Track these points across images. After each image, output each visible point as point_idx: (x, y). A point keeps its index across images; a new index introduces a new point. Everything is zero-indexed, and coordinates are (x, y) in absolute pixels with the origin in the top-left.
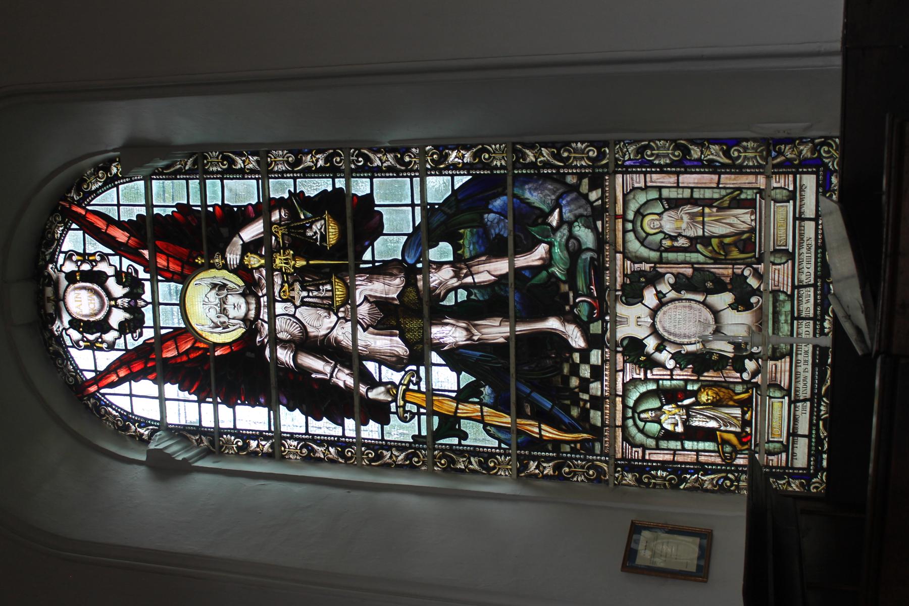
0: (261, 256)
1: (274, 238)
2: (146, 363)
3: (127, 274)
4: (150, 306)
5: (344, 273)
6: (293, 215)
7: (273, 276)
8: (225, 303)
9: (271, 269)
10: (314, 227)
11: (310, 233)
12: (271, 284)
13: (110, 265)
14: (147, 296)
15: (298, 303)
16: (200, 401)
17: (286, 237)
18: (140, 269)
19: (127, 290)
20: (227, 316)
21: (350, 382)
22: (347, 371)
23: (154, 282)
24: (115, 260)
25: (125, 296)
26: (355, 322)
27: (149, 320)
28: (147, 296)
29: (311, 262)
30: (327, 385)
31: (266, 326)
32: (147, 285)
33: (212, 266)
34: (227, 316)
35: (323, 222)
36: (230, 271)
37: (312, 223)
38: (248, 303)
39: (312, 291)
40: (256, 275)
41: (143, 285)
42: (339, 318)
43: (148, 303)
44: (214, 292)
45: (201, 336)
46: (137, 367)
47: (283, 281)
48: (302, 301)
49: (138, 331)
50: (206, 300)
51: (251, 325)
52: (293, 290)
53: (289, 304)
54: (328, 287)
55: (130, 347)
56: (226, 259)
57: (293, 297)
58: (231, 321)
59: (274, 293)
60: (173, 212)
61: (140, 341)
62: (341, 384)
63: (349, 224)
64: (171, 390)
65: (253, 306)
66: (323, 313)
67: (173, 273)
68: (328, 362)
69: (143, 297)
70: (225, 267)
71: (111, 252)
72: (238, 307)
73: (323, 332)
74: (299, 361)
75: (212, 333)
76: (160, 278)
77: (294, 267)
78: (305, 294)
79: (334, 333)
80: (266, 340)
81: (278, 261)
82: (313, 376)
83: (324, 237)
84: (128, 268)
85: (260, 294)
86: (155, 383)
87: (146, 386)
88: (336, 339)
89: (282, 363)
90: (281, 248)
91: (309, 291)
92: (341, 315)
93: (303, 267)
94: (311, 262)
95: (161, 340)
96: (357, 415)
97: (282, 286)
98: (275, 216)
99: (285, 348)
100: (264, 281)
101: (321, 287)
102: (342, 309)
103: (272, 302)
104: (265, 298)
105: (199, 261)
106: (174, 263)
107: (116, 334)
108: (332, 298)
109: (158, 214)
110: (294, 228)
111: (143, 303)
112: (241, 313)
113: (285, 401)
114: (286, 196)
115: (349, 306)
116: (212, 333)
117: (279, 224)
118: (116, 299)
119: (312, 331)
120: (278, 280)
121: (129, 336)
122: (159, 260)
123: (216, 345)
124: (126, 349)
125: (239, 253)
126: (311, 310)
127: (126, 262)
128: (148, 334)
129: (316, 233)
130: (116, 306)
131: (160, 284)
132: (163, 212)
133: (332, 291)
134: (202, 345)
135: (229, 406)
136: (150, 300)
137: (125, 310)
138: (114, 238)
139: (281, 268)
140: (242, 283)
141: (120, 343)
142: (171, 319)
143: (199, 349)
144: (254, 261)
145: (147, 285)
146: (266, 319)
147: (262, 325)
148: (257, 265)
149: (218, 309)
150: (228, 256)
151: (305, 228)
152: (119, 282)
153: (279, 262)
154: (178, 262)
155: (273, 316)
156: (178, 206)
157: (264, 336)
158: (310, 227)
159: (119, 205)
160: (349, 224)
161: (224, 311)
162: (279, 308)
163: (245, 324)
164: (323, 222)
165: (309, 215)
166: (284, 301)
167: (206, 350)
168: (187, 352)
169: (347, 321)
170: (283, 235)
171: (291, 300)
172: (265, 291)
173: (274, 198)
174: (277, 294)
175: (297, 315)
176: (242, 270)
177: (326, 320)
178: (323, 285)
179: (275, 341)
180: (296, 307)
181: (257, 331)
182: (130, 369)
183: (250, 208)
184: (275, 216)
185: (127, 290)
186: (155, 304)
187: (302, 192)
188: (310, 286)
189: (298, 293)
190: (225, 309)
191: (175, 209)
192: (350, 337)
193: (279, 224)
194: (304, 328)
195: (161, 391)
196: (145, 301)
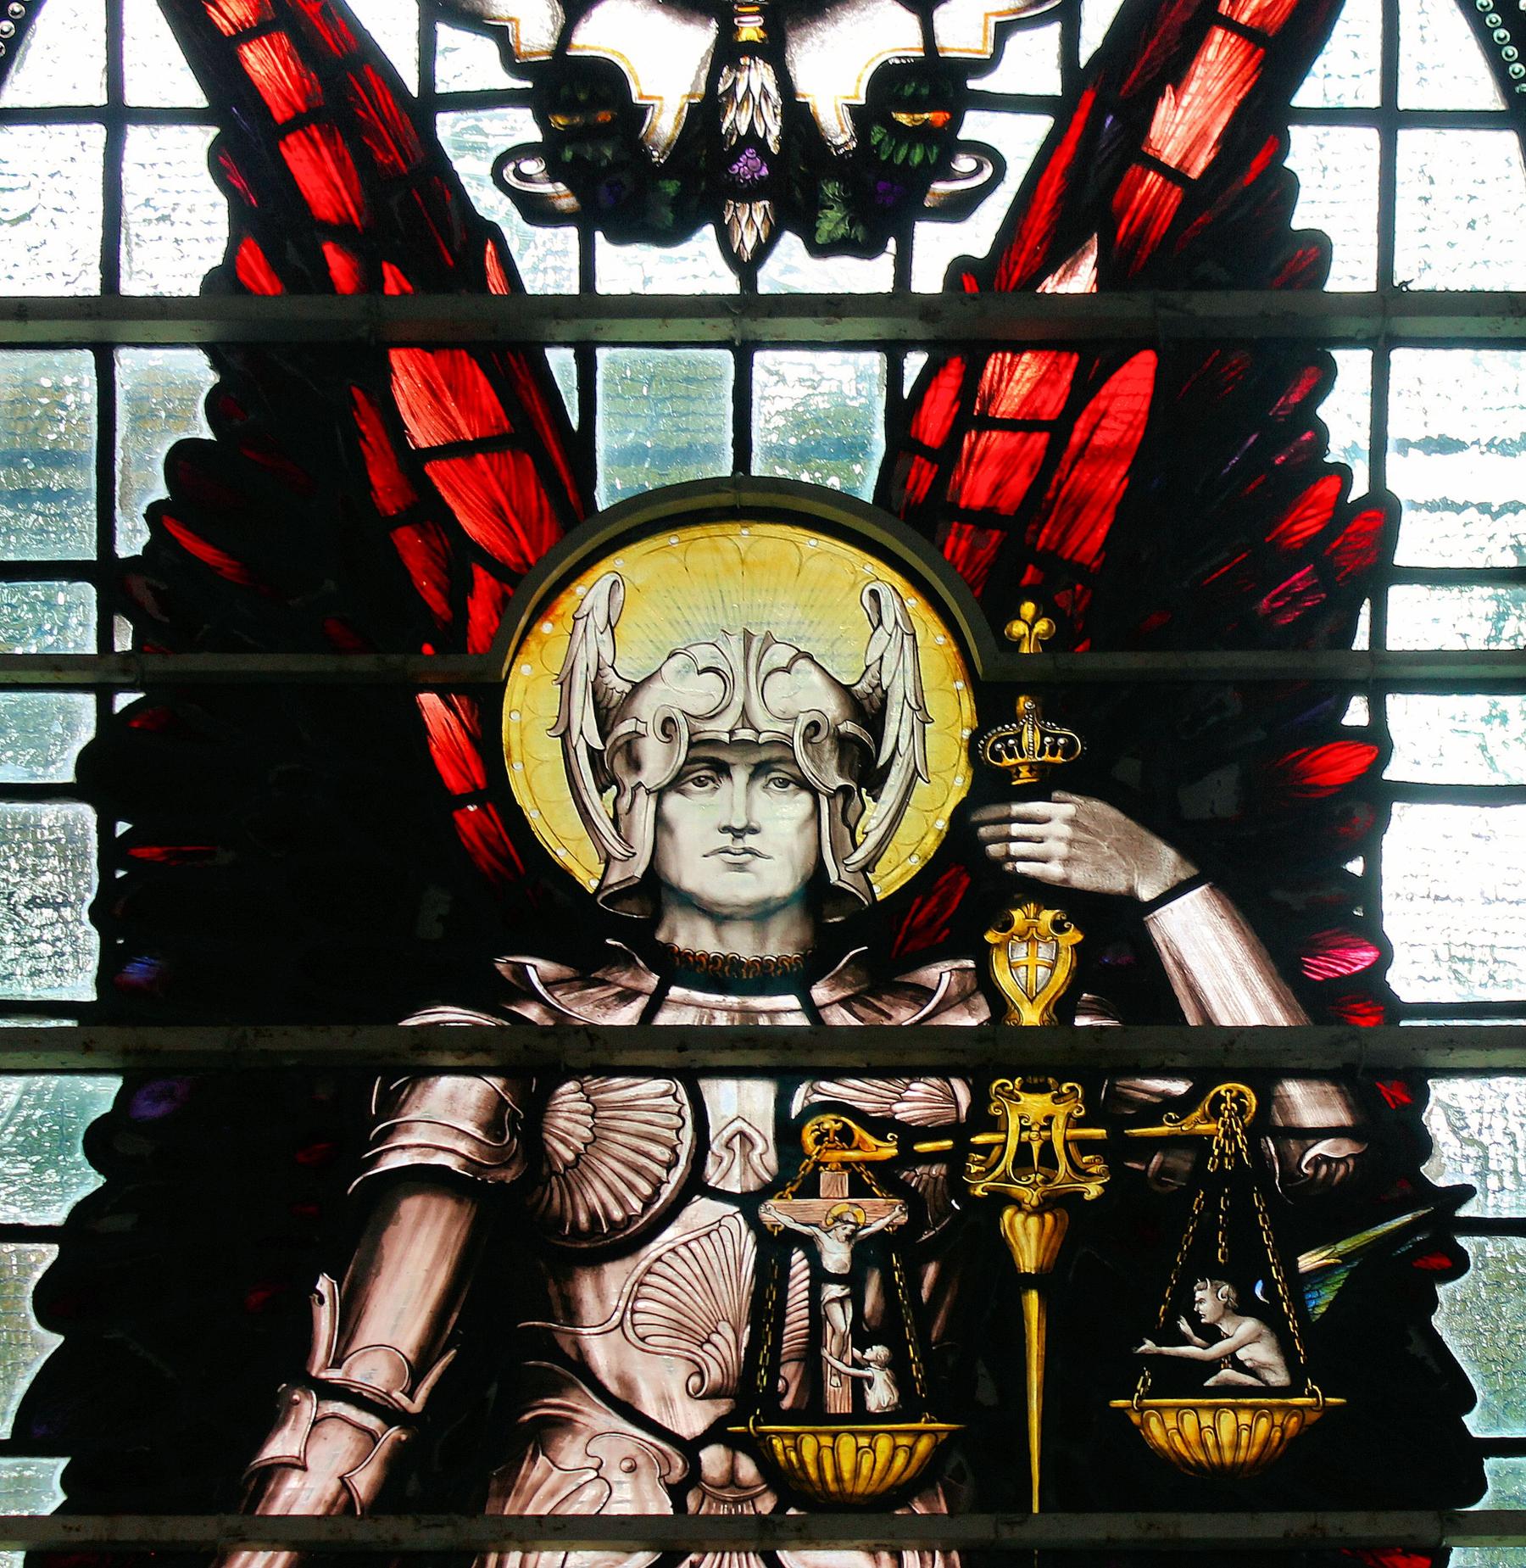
0: (1064, 1007)
1: (1179, 1087)
2: (342, 232)
3: (947, 143)
4: (729, 284)
5: (966, 1491)
6: (1319, 1209)
7: (944, 1073)
8: (759, 770)
9: (994, 1057)
10: (1249, 1325)
11: (1208, 1300)
12: (893, 1058)
13: (1003, 31)
14: (792, 268)
15: (778, 1213)
16: (107, 575)
17: (1182, 1162)
18: (976, 235)
19: (837, 129)
20: (676, 784)
21: (300, 1498)
22: (364, 1482)
23: (885, 323)
24: (1034, 64)
25: (797, 116)
26: (668, 1540)
27: (627, 269)
28: (792, 268)
29: (1033, 1300)
30: (273, 1367)
31: (627, 1015)
32: (870, 276)
33: (993, 705)
34: (676, 784)
35: (1278, 1378)
36: (960, 816)
37: (1270, 1316)
38: (761, 914)
39: (857, 1299)
40: (941, 975)
41: (868, 249)
42: (690, 1448)
43: (746, 269)
44: (831, 707)
45: (543, 610)
46: (314, 172)
47: (908, 1133)
48: (791, 1239)
49: (560, 194)
50: (780, 655)
51: (627, 924)
52: (859, 1189)
53: (765, 1159)
54: (881, 1395)
55: (447, 126)
56: (1039, 792)
57: (810, 1189)
58: (645, 810)
59: (833, 1075)
60: (1343, 473)
61: (490, 203)
62: (281, 1446)
63: (1272, 1526)
64: (173, 384)
65: (741, 944)
66: (725, 1351)
67: (947, 455)
68: (417, 1371)
69: (790, 243)
70: (991, 785)
71: (1091, 39)
72: (742, 853)
73: (602, 1353)
74: (411, 1206)
75: (565, 682)
76: (915, 362)
77: (1001, 1200)
78: (836, 1256)
79: (597, 1417)
80: (533, 1012)
81: (1035, 1105)
82: (324, 1284)
83: (1186, 1380)
84: (984, 151)
85: (820, 993)
86: (212, 281)
87: (184, 231)
88: (563, 1425)
89: (392, 1104)
90: (1115, 1125)
91: (853, 1280)
92: (713, 1459)
93: (1003, 1251)
94: (1033, 1300)
95: (508, 344)
96: (92, 1528)
97: (880, 1126)
98: (1309, 1104)
99: (493, 1126)
100: (905, 1016)
101: (878, 1352)
102: (747, 1469)
103: (781, 1059)
104: (799, 1020)
105: (1029, 627)
106: (1009, 461)
107: (536, 32)
108: (813, 1411)
109: (1326, 376)
110: (1242, 1217)
111: (747, 239)
112: (696, 869)
113: (148, 1109)
114: (1442, 1172)
115: (766, 1505)
116: (565, 682)
117: (1261, 1126)
118: (774, 51)
119: (604, 1291)
120: (916, 1101)
121: (522, 126)
122: (1028, 368)
123: (484, 701)
124: (433, 102)
125: (1082, 878)
126: (733, 1291)
127: (1020, 139)
128: (545, 260)
129: (1211, 1334)
130: (727, 53)
131: (874, 362)
132: (1343, 416)
133: (860, 1413)
134: (480, 611)
135: (86, 759)
136: (769, 280)
137: (706, 112)
138: (1175, 73)
139: (995, 1125)
140: (888, 880)
141: (468, 61)
142: (640, 419)
143: (458, 590)
144: (1033, 966)
145: (870, 276)
146: (664, 1018)
147: (627, 996)
148: (1004, 979)
149: (719, 729)
150: (1059, 812)
151: (1240, 1273)
152: (890, 83)
153: (1032, 1111)
154: (1019, 483)
155: (691, 1060)
156: (1382, 512)
157: (562, 999)
158: (1244, 1306)
159: (1389, 118)
160: (1272, 1526)
161: (707, 762)
162: (742, 1103)
163: (629, 892)
164: (1278, 1378)
165: (1321, 1302)
166: (787, 1132)
167: (453, 637)
168: (432, 514)
169: (677, 1493)
170: (1200, 1144)
171: (795, 1173)
172: (839, 1017)
173: (1421, 1097)
174: (832, 1089)
175: (702, 1210)
176: (967, 891)
177: (676, 1376)
178: (897, 1367)
179: (533, 1068)
180: (749, 1203)
181: (587, 968)
182: (297, 123)
183: (1366, 957)
184: (1309, 1104)
185: (837, 129)
186: (748, 322)
187: (1458, 1264)
188: (887, 1287)
189: (837, 1223)
190: (722, 770)
191: (1360, 488)
192: (583, 1505)
193: (1261, 1126)
194: (625, 1240)
195: (158, 318)
196: (763, 250)
